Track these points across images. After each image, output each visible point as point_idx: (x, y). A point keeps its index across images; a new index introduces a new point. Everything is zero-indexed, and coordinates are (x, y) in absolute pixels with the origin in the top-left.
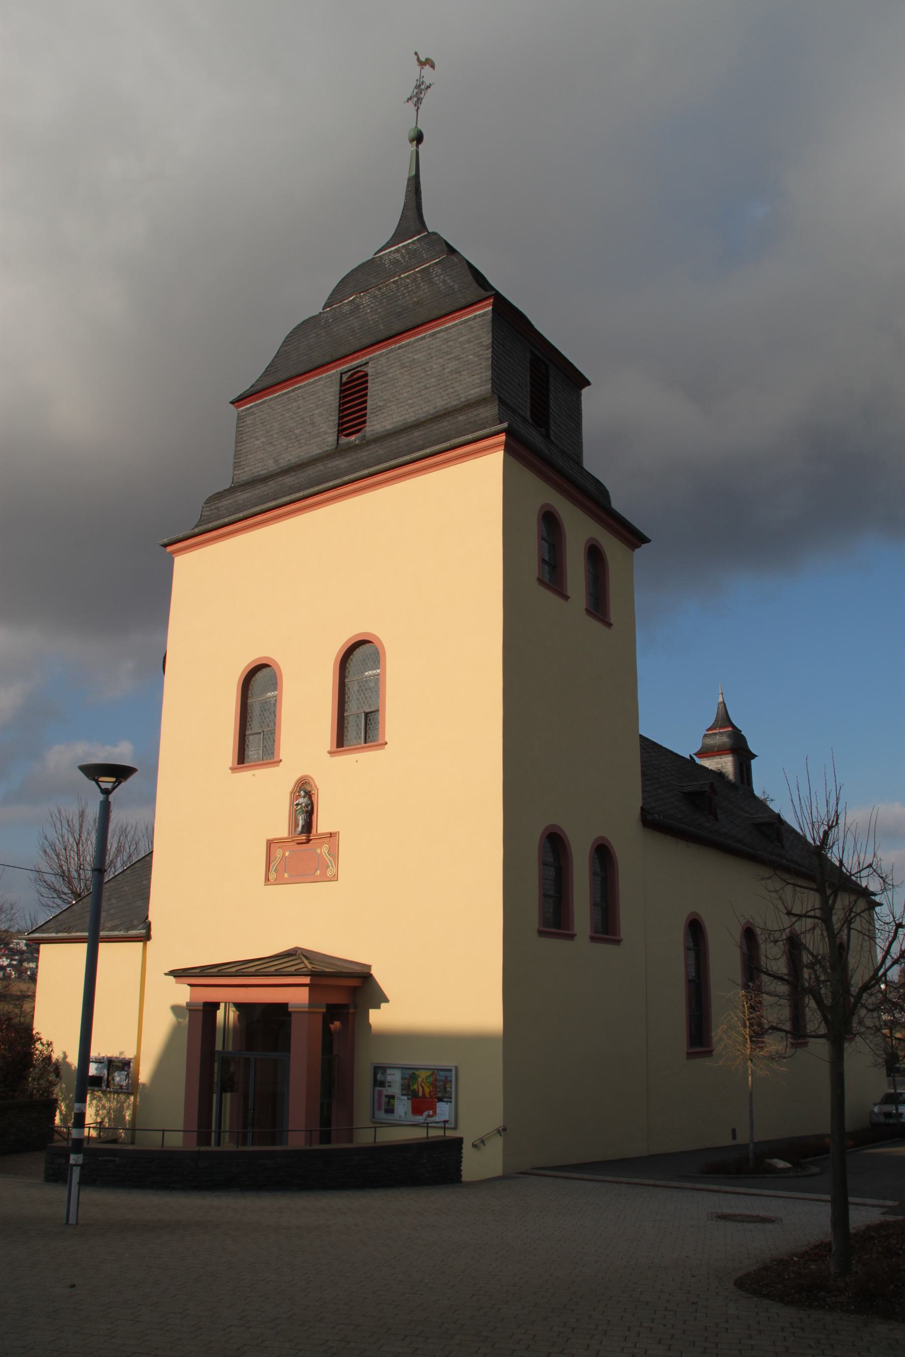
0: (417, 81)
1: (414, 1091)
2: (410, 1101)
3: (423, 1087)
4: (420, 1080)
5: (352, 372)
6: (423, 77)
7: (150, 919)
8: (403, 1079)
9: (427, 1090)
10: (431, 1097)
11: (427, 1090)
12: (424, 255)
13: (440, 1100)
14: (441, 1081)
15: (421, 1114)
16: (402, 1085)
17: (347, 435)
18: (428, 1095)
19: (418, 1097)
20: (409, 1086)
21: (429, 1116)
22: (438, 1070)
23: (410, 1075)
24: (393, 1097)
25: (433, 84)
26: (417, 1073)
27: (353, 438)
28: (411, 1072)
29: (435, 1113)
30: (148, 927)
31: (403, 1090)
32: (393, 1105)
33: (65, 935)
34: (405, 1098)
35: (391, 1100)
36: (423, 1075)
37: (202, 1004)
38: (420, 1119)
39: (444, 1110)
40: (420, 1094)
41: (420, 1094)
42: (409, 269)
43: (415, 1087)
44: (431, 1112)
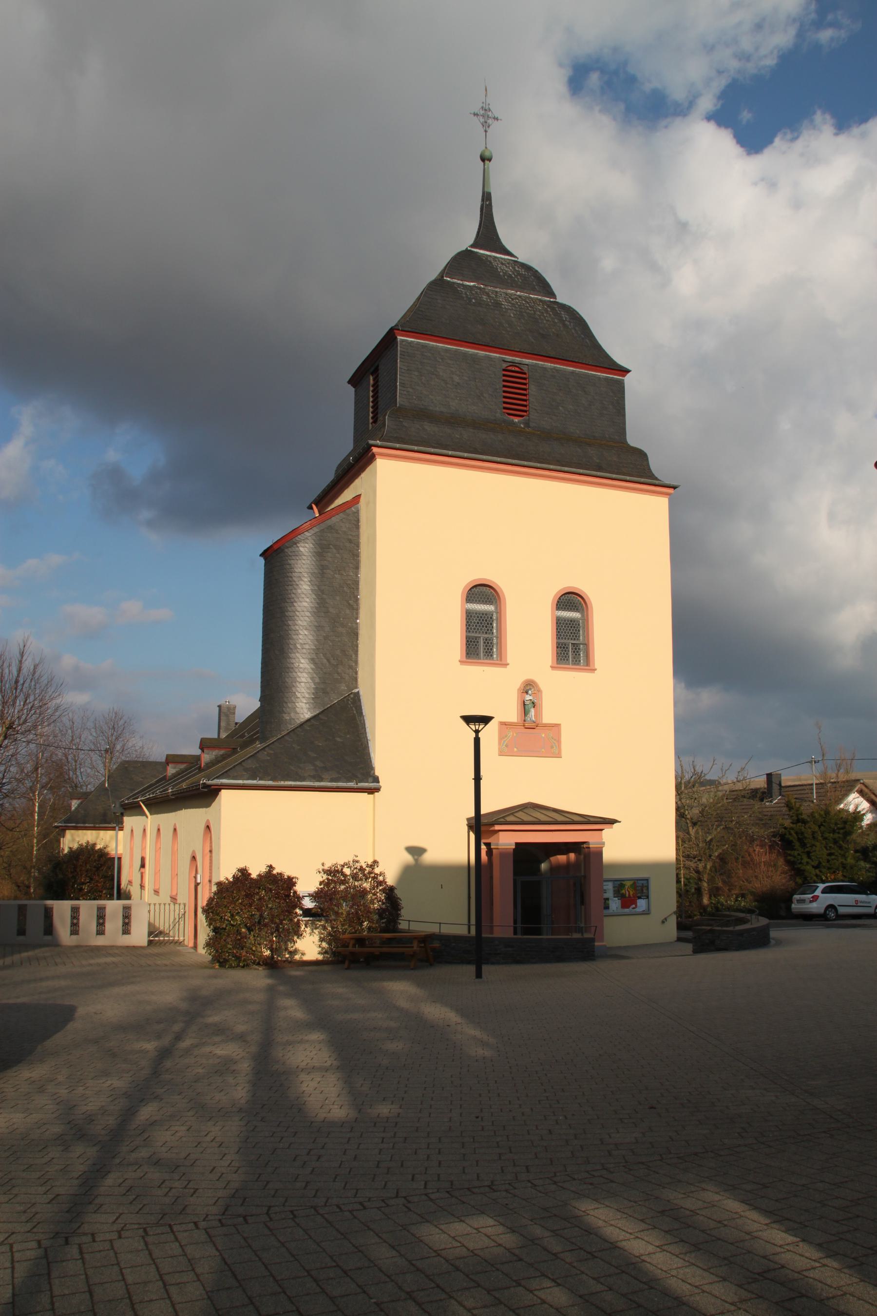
0: (483, 103)
1: (623, 893)
2: (620, 901)
3: (628, 891)
4: (626, 887)
5: (511, 364)
6: (489, 104)
7: (377, 774)
8: (614, 887)
9: (631, 893)
10: (634, 897)
11: (631, 893)
12: (536, 287)
13: (640, 898)
14: (640, 886)
15: (628, 907)
16: (614, 891)
17: (509, 414)
18: (632, 896)
19: (625, 897)
20: (619, 891)
21: (634, 908)
22: (637, 880)
23: (619, 885)
24: (608, 899)
25: (501, 120)
26: (624, 883)
27: (516, 420)
28: (619, 883)
29: (636, 906)
30: (376, 780)
31: (614, 894)
32: (609, 904)
33: (270, 783)
34: (617, 899)
35: (607, 901)
36: (628, 884)
37: (514, 844)
38: (626, 910)
39: (642, 904)
40: (627, 896)
41: (627, 896)
42: (525, 291)
43: (623, 891)
44: (634, 906)
